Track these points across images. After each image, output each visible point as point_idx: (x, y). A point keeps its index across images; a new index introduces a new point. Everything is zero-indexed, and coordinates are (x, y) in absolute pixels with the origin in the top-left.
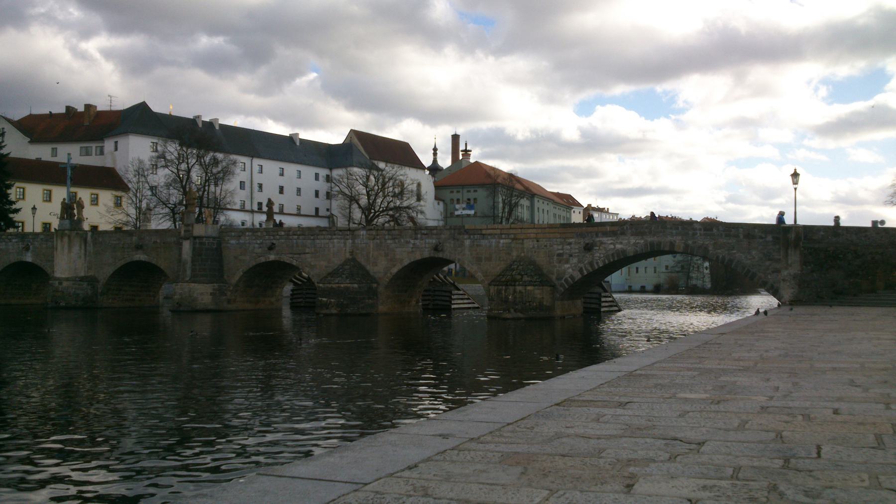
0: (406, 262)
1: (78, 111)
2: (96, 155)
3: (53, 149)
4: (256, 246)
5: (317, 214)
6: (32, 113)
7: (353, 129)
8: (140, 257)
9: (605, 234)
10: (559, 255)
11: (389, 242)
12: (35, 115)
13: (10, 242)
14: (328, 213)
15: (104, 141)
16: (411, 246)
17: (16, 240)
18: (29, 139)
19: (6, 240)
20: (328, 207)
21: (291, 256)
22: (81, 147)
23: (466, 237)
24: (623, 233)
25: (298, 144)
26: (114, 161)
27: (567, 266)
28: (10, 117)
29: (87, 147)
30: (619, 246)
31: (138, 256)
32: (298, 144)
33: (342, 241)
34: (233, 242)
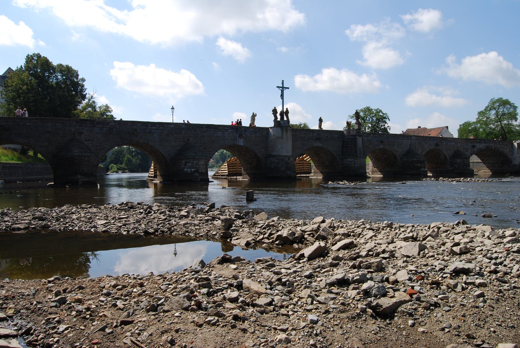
0: (427, 150)
4: (375, 141)
8: (317, 145)
9: (477, 143)
10: (466, 149)
11: (422, 142)
13: (227, 131)
16: (429, 144)
17: (232, 131)
19: (223, 130)
21: (389, 146)
23: (444, 141)
24: (481, 143)
27: (468, 153)
30: (480, 147)
31: (317, 144)
33: (407, 140)
34: (365, 139)
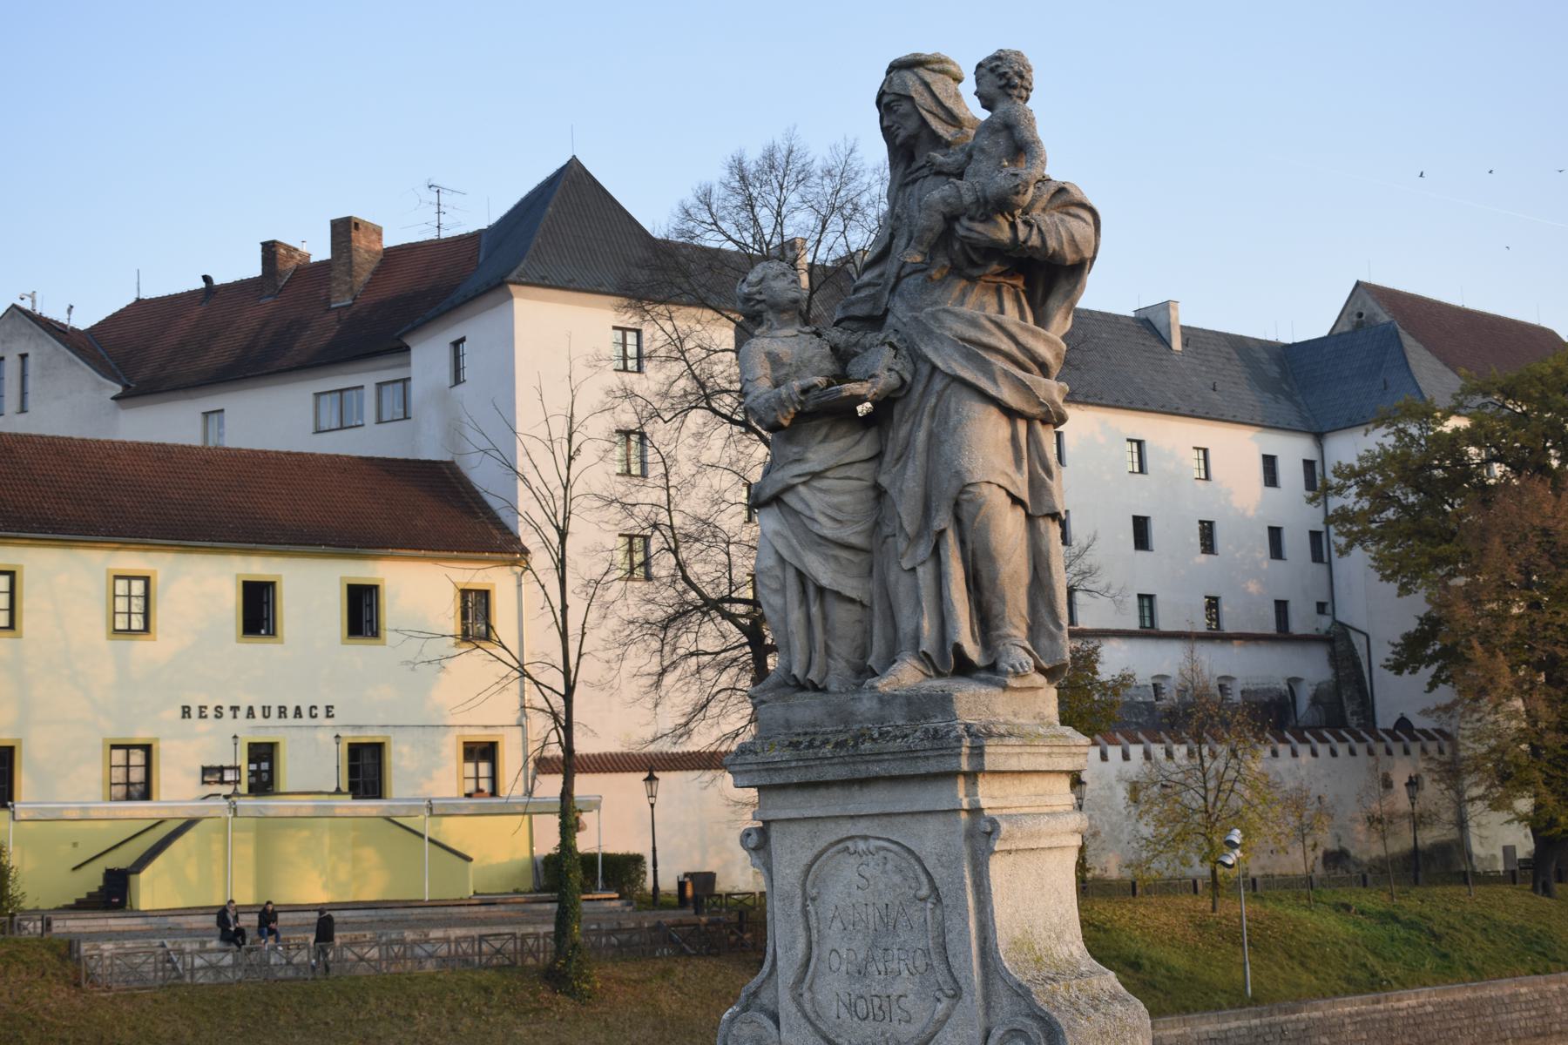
1: (313, 260)
2: (380, 421)
3: (206, 414)
5: (1283, 634)
6: (141, 297)
7: (1365, 279)
12: (151, 300)
14: (1325, 623)
15: (408, 349)
18: (118, 389)
20: (1324, 598)
22: (317, 395)
25: (1177, 344)
26: (454, 431)
28: (52, 310)
29: (341, 391)
32: (1177, 344)
